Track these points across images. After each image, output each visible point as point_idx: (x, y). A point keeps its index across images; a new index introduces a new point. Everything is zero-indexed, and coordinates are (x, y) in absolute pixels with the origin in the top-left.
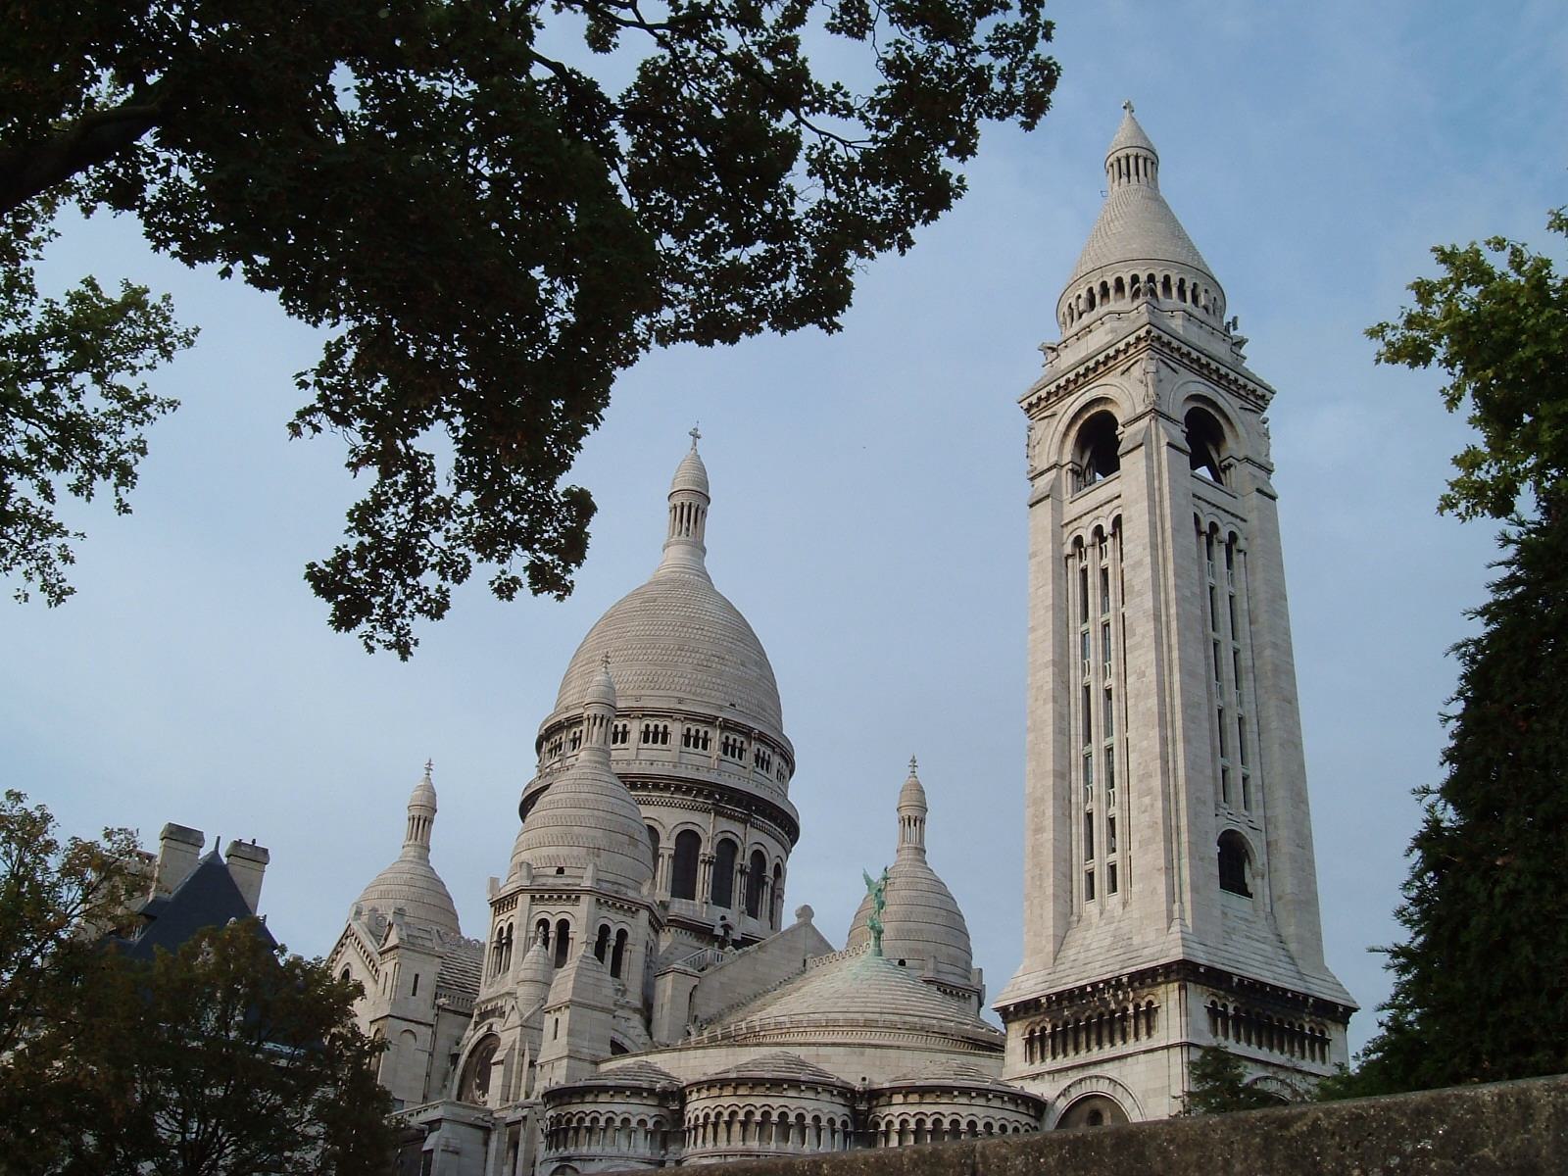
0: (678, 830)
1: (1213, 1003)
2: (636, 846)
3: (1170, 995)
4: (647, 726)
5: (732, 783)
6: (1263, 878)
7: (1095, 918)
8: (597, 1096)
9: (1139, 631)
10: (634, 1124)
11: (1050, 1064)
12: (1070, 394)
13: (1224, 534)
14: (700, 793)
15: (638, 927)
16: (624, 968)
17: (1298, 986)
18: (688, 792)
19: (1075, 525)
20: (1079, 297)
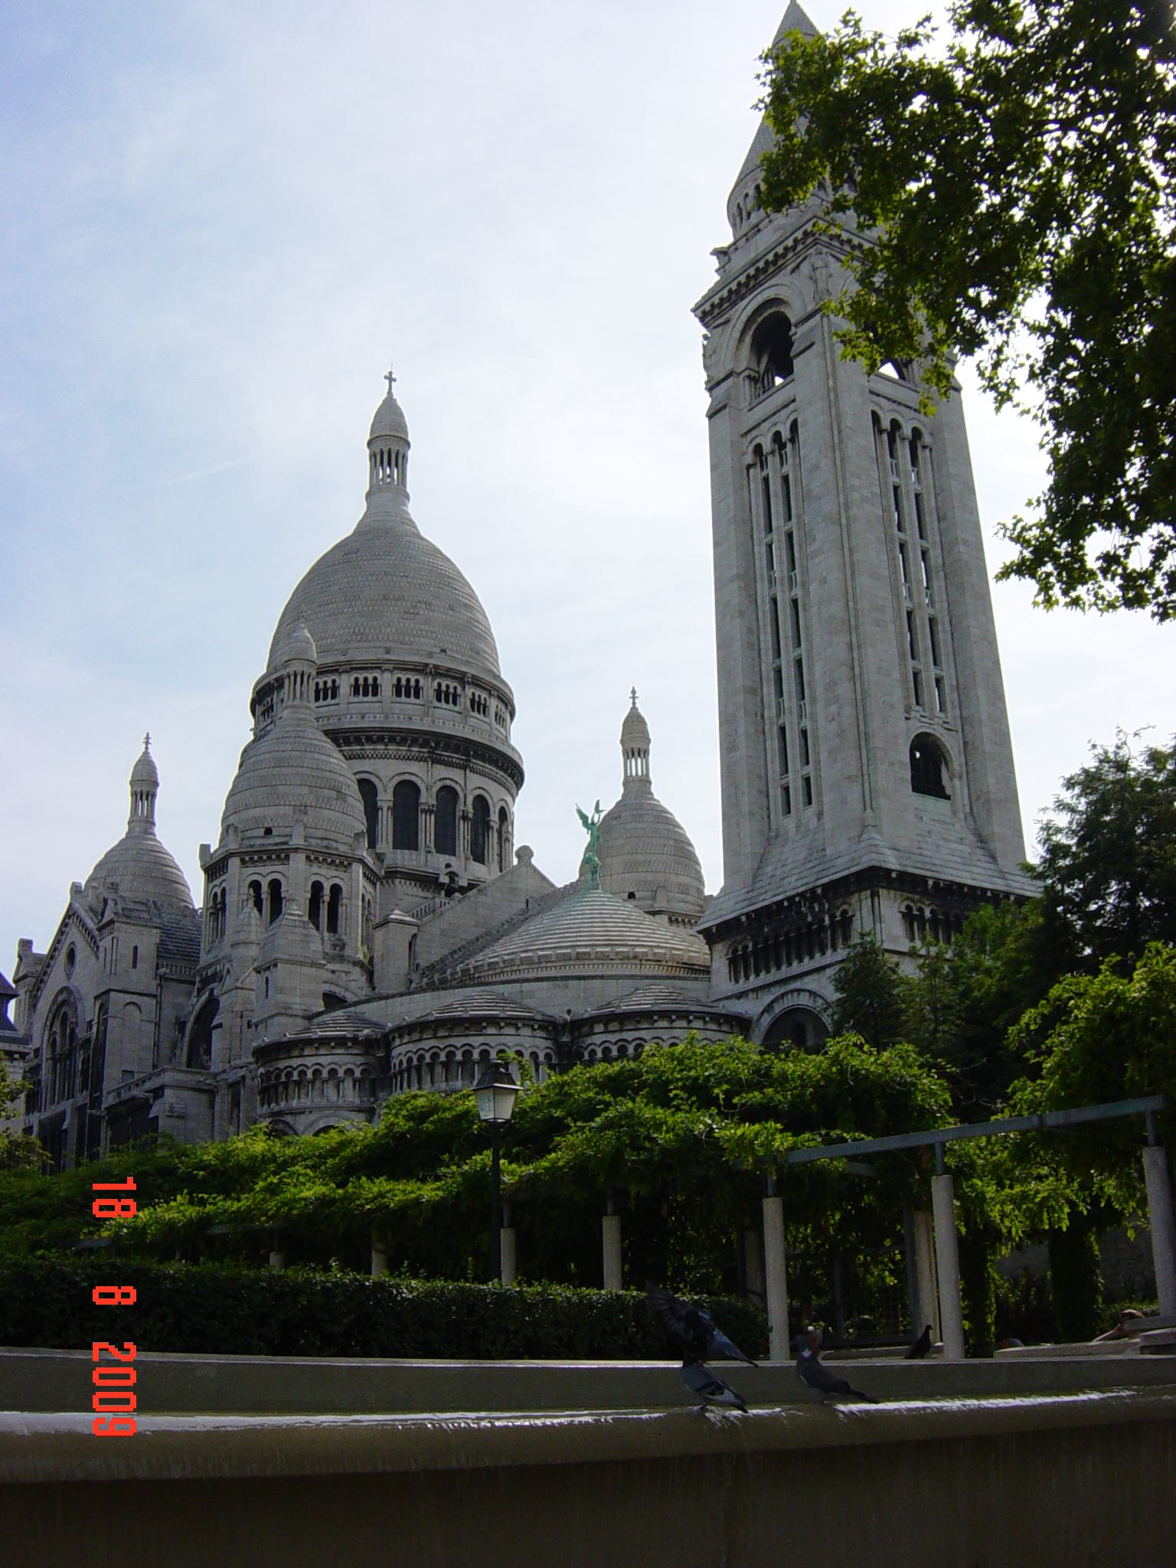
0: (395, 781)
1: (908, 907)
3: (864, 903)
4: (357, 680)
5: (447, 729)
6: (961, 778)
7: (792, 831)
9: (819, 536)
10: (341, 1073)
11: (754, 981)
12: (743, 298)
13: (907, 431)
14: (414, 742)
15: (356, 883)
16: (341, 922)
17: (999, 885)
18: (403, 741)
19: (754, 433)
20: (747, 195)
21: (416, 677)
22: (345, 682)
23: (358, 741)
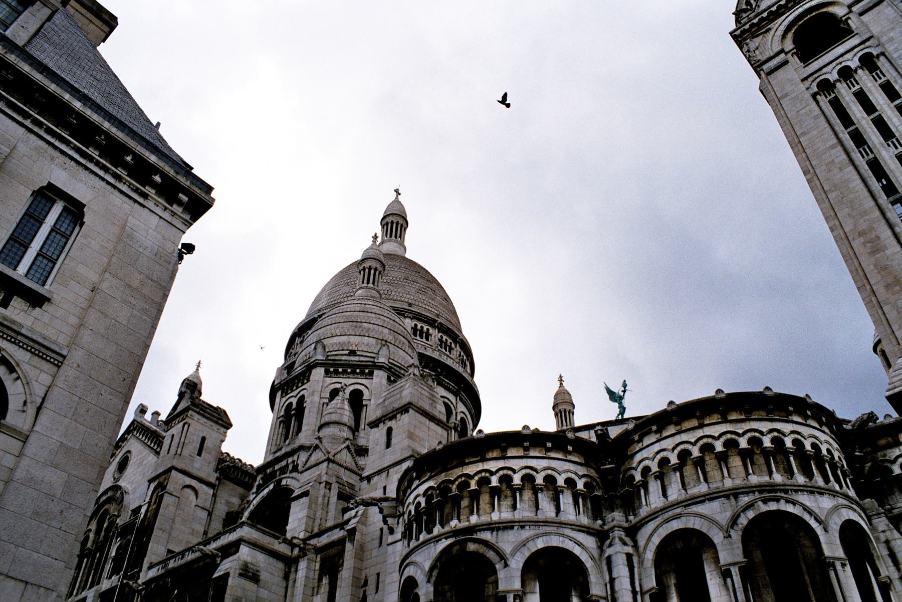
5: (449, 362)
8: (504, 450)
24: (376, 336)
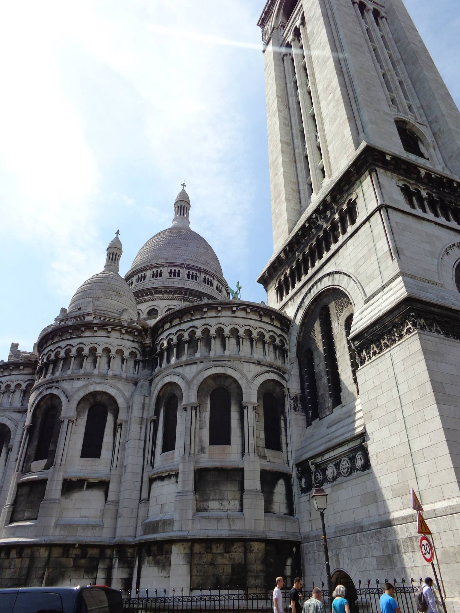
2: (121, 297)
4: (153, 272)
10: (13, 387)
14: (176, 292)
18: (170, 292)
21: (178, 269)
22: (149, 273)
23: (151, 294)
24: (92, 296)
